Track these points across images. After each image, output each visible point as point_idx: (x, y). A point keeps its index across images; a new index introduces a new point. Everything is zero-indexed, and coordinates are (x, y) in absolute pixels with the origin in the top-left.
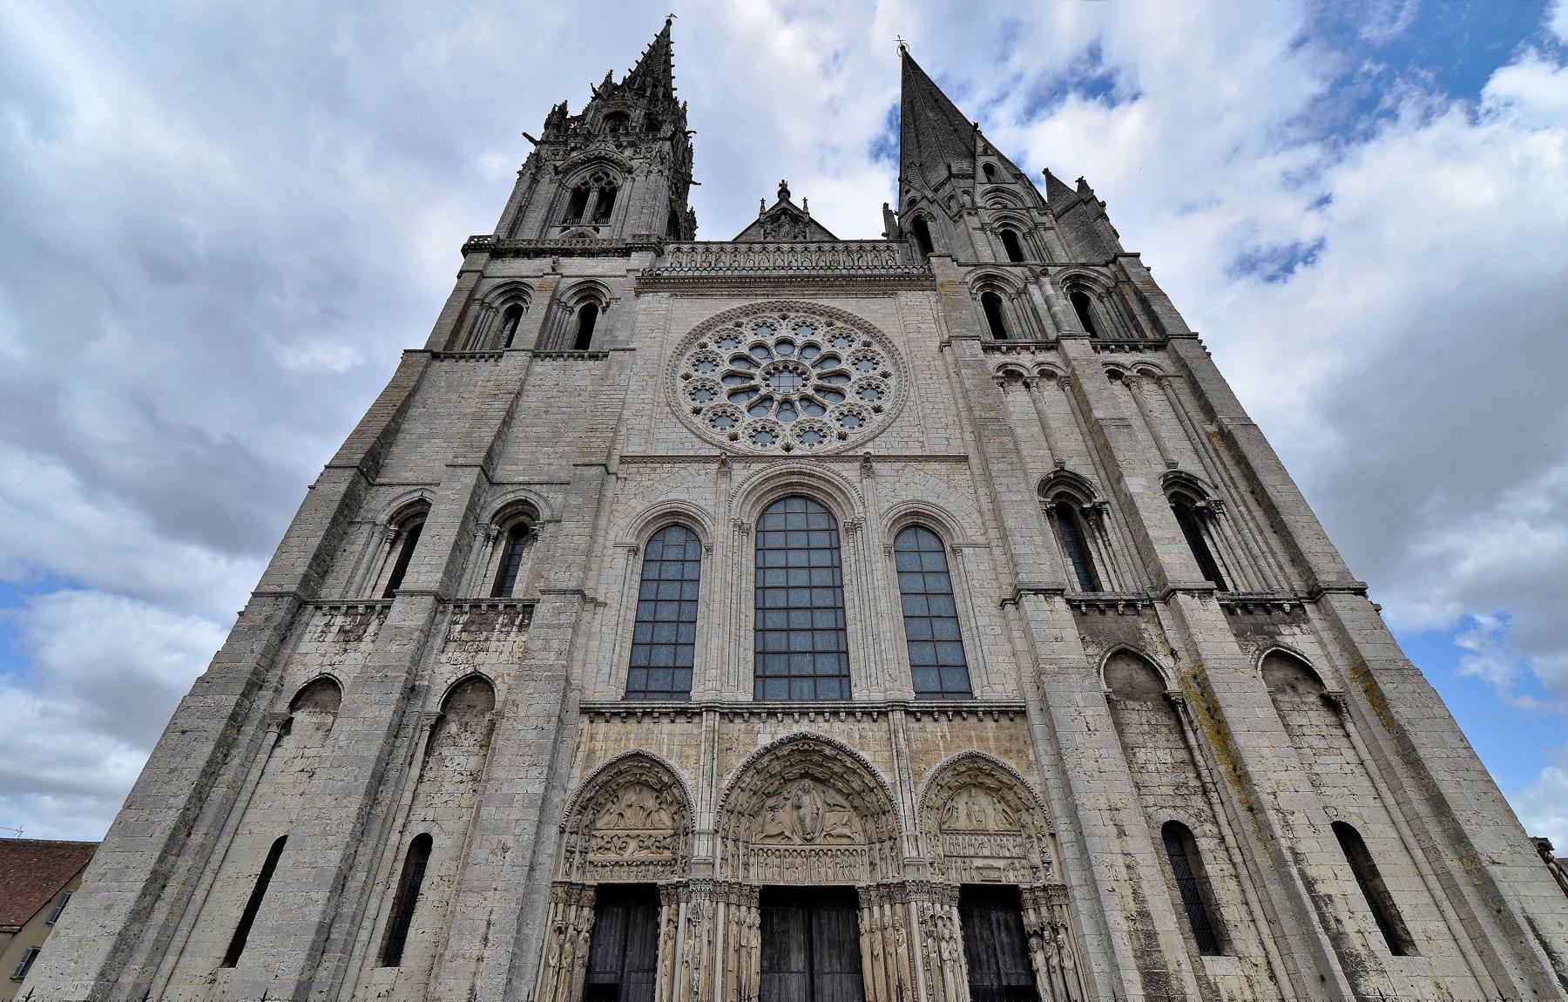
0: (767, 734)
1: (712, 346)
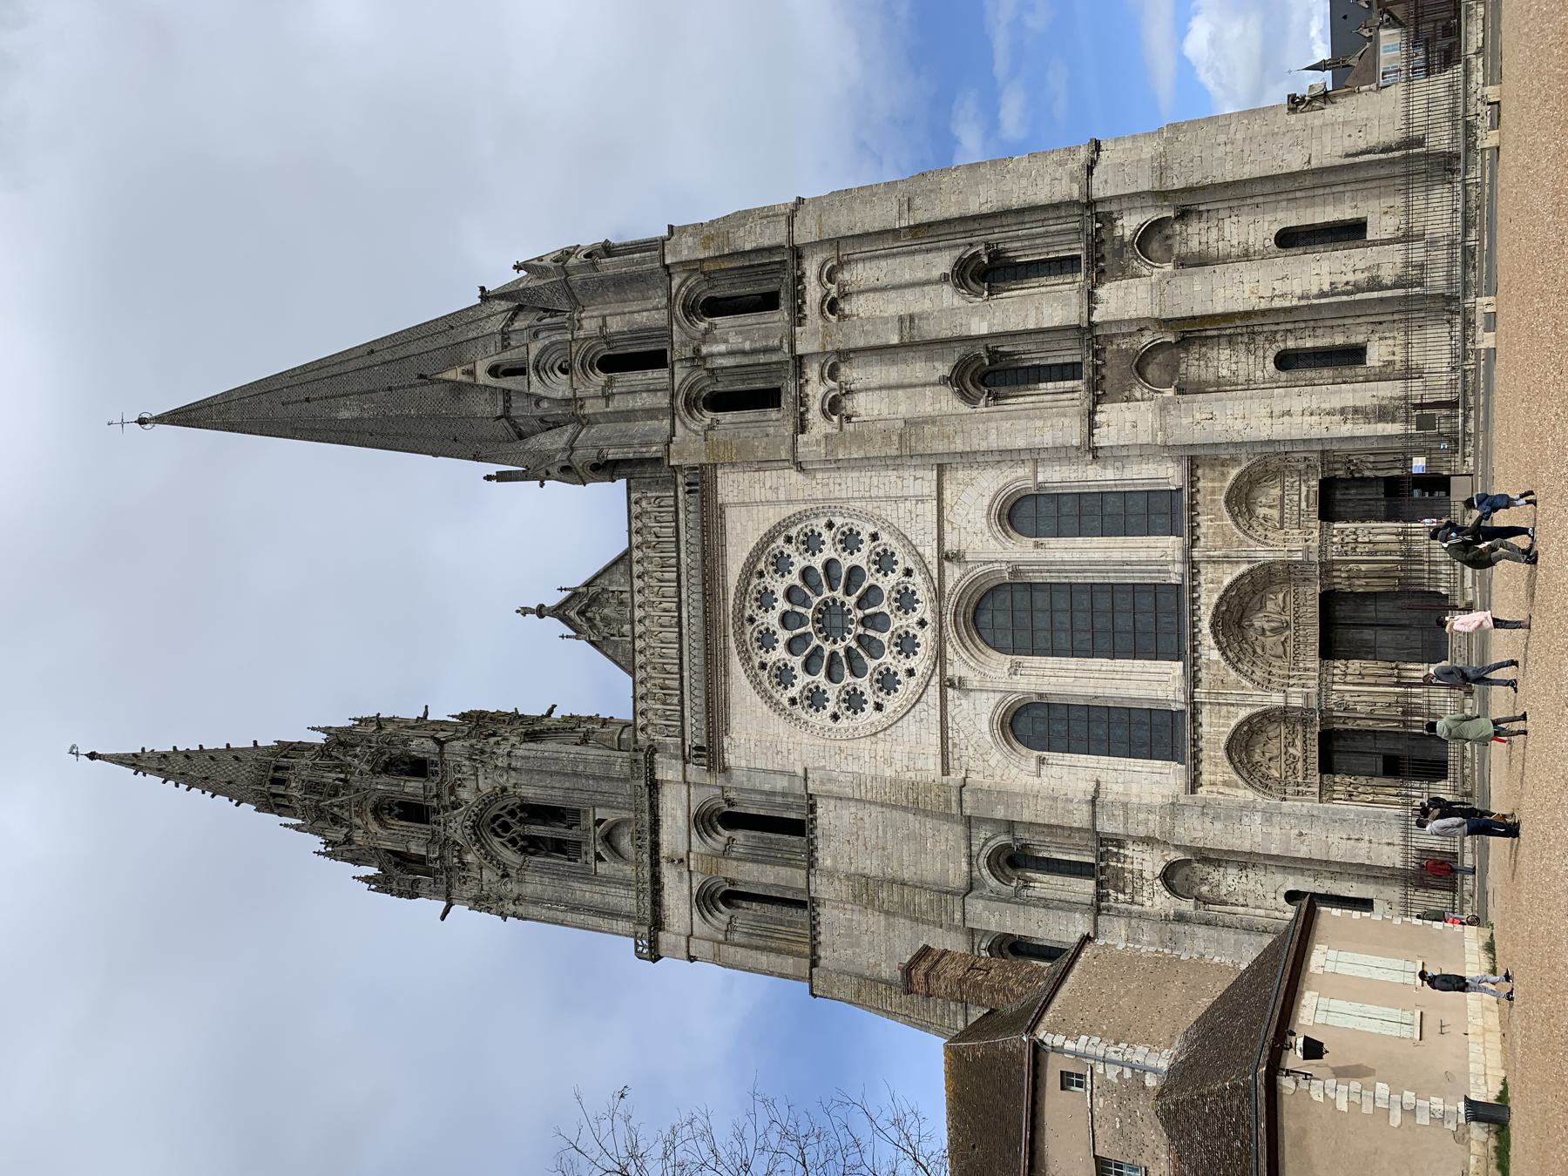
0: (1210, 651)
1: (793, 692)
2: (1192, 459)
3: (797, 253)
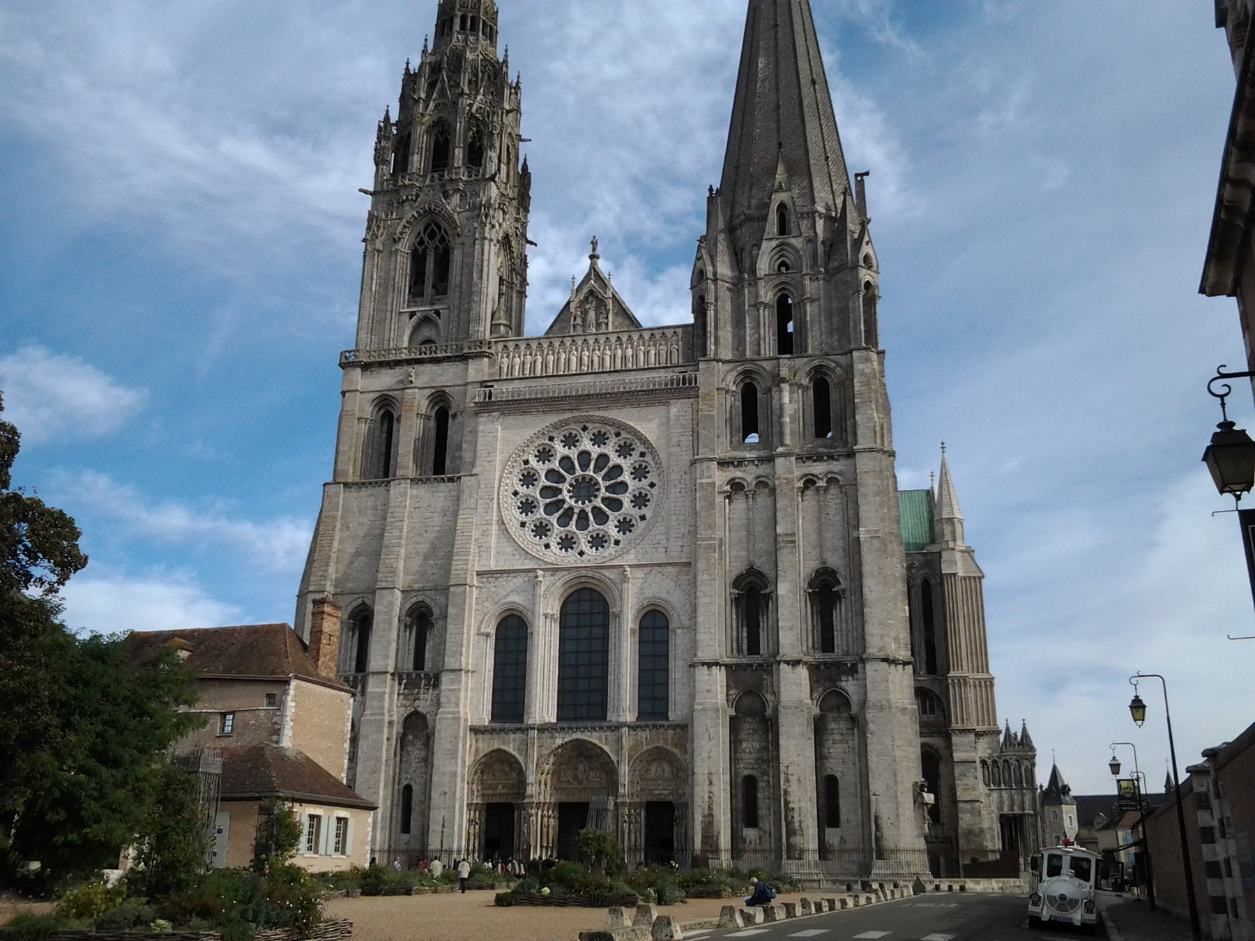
1: (533, 462)
2: (686, 726)
3: (851, 455)
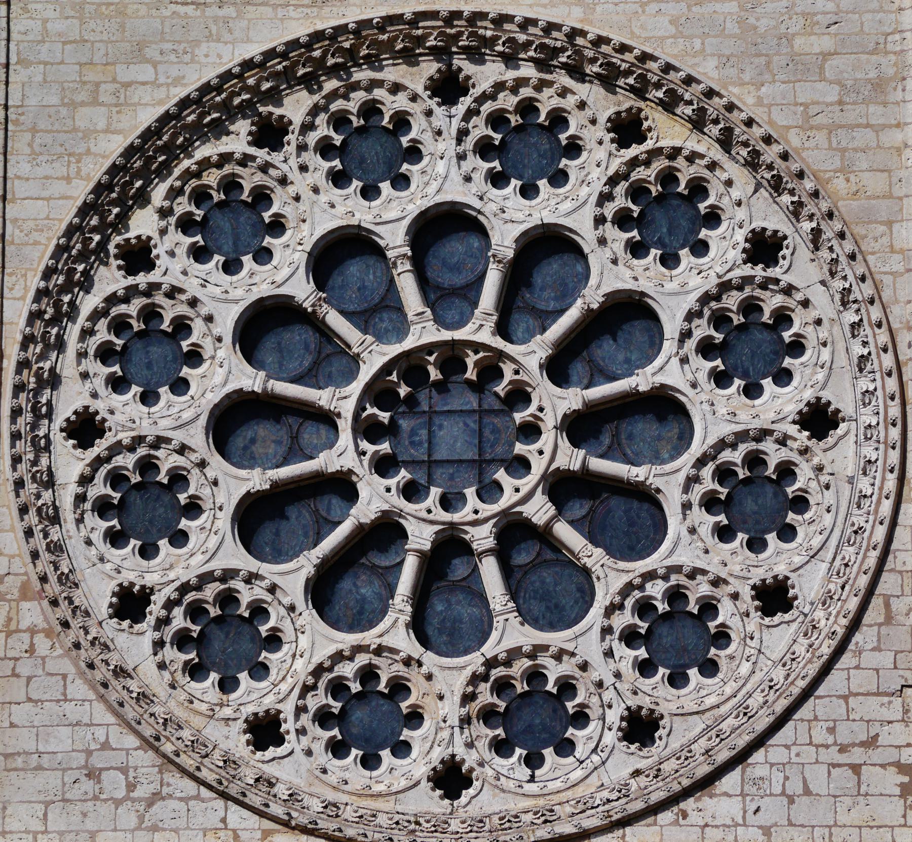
1: (173, 262)
